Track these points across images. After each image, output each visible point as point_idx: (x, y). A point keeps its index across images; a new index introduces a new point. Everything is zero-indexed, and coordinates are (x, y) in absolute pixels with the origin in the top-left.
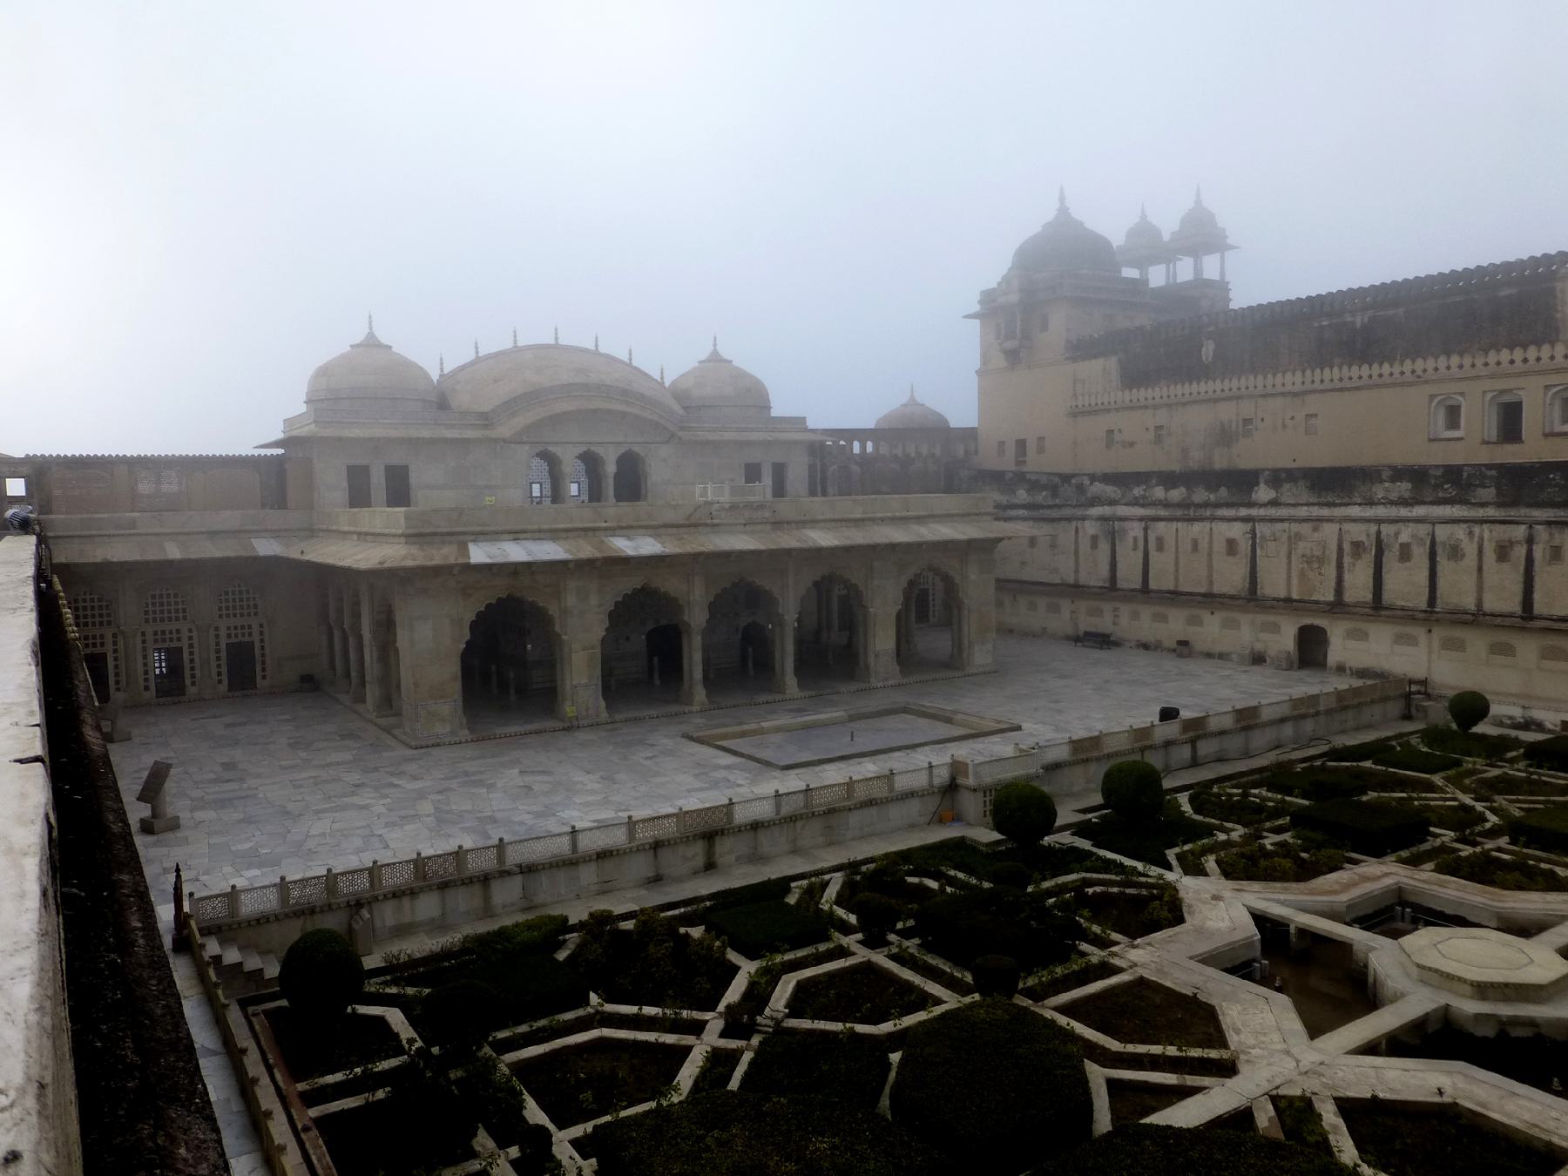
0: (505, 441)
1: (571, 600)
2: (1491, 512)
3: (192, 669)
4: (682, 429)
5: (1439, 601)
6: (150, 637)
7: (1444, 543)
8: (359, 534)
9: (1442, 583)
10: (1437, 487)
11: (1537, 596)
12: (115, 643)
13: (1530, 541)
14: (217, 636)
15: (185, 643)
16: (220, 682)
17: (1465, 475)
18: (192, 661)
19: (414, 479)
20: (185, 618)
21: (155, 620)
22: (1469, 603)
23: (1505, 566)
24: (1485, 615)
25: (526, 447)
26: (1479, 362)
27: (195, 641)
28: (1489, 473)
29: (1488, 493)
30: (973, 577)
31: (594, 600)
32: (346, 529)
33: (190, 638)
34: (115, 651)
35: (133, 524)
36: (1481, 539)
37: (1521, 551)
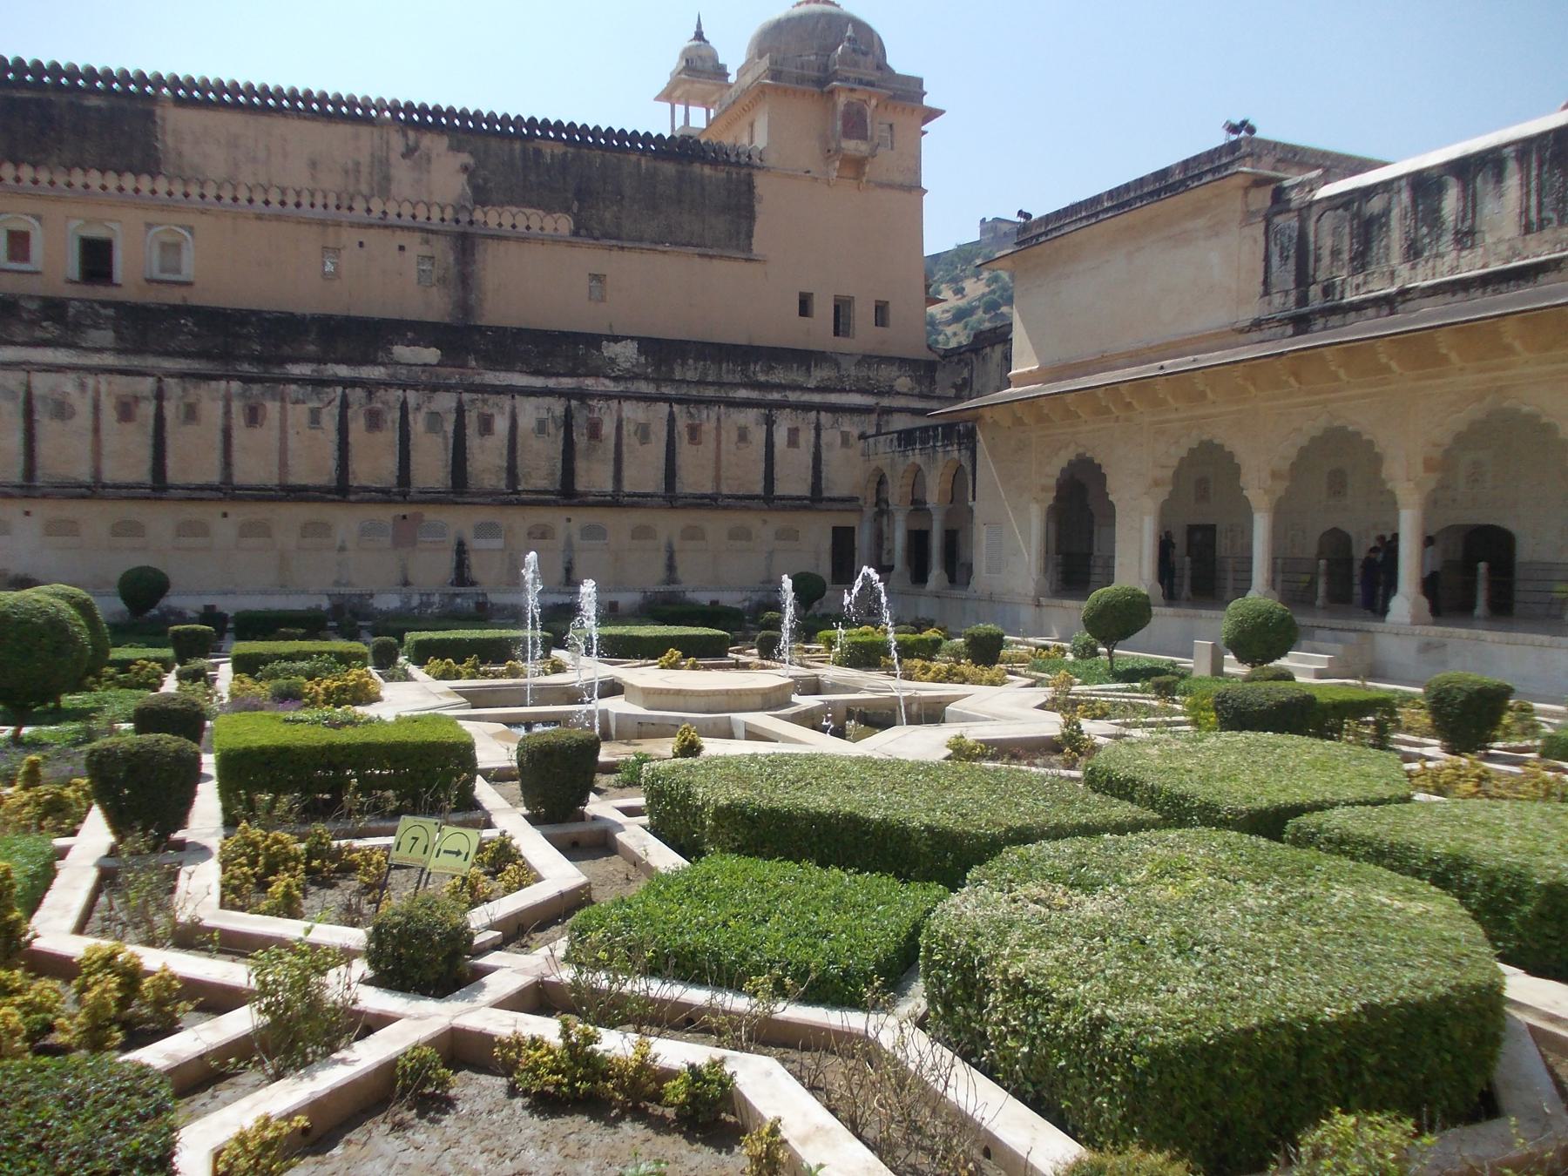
2: (109, 360)
5: (39, 473)
7: (44, 398)
9: (44, 448)
10: (33, 323)
11: (171, 463)
13: (160, 396)
17: (71, 311)
22: (83, 473)
23: (130, 427)
24: (105, 486)
26: (61, 180)
28: (102, 311)
29: (106, 336)
36: (97, 392)
37: (147, 410)
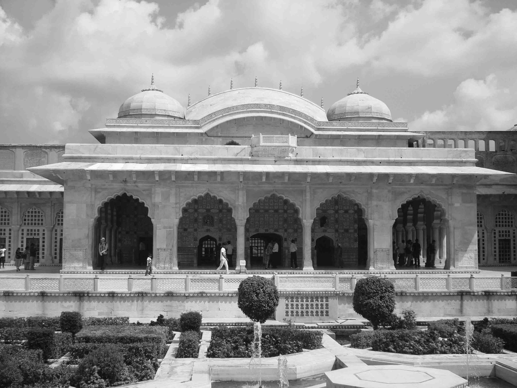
1: (158, 199)
3: (43, 250)
4: (318, 129)
6: (25, 232)
12: (10, 234)
14: (56, 234)
15: (41, 237)
16: (56, 258)
18: (43, 246)
20: (42, 224)
21: (28, 224)
25: (220, 139)
27: (46, 236)
30: (457, 205)
31: (172, 200)
33: (44, 234)
34: (10, 238)
35: (22, 176)
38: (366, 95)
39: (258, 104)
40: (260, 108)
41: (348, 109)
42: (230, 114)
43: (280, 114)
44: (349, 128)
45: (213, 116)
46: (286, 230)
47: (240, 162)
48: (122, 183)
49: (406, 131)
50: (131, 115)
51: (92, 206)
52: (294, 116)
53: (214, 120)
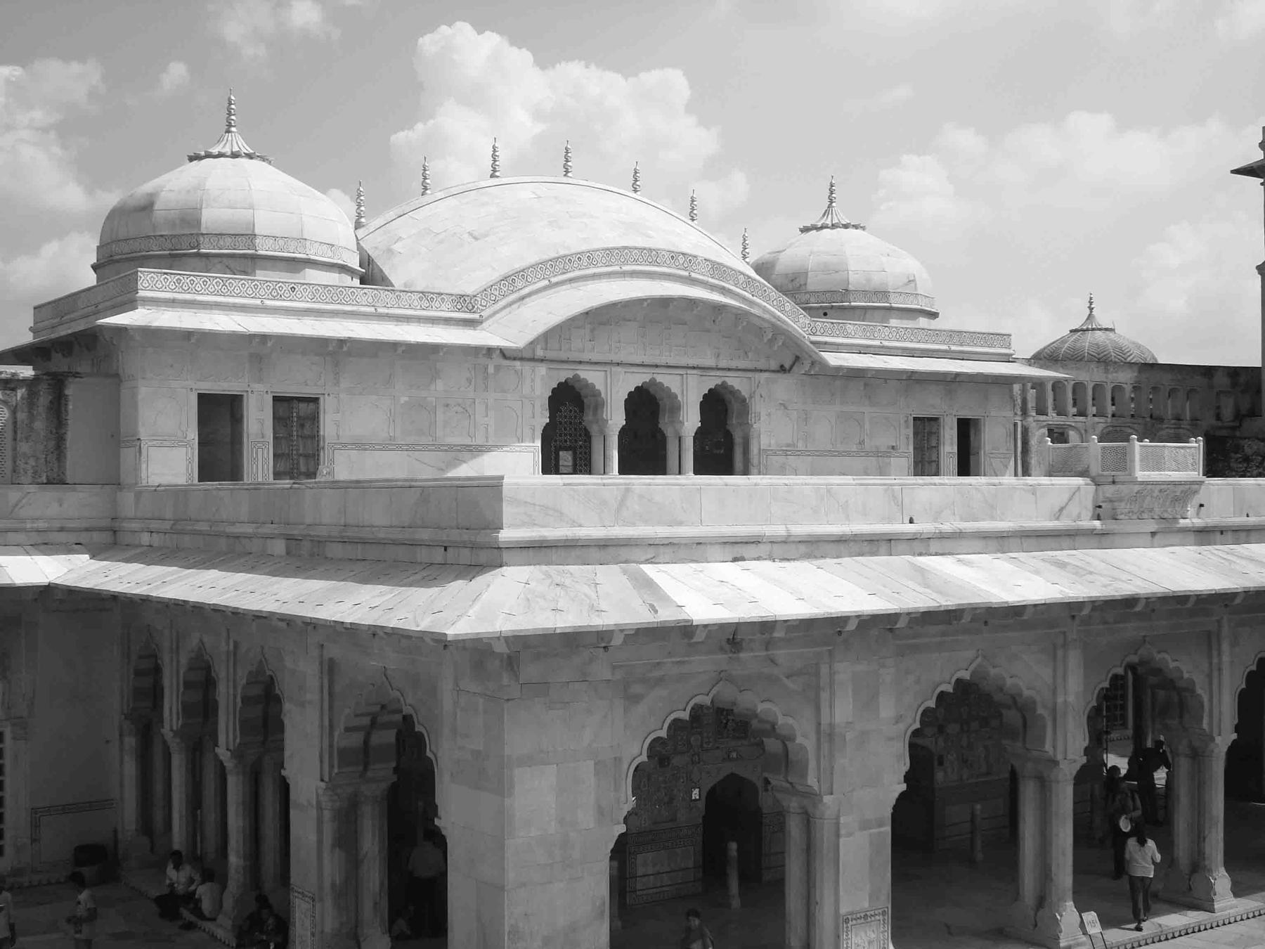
0: (504, 353)
1: (842, 710)
8: (289, 538)
19: (329, 426)
25: (542, 369)
31: (887, 708)
32: (249, 529)
38: (859, 231)
39: (650, 250)
40: (659, 265)
41: (855, 280)
42: (571, 280)
43: (713, 288)
44: (886, 343)
45: (519, 284)
46: (941, 729)
47: (1066, 542)
48: (722, 649)
49: (1008, 359)
50: (207, 256)
51: (618, 760)
52: (749, 296)
53: (523, 298)
